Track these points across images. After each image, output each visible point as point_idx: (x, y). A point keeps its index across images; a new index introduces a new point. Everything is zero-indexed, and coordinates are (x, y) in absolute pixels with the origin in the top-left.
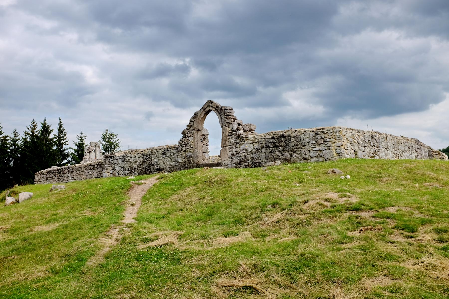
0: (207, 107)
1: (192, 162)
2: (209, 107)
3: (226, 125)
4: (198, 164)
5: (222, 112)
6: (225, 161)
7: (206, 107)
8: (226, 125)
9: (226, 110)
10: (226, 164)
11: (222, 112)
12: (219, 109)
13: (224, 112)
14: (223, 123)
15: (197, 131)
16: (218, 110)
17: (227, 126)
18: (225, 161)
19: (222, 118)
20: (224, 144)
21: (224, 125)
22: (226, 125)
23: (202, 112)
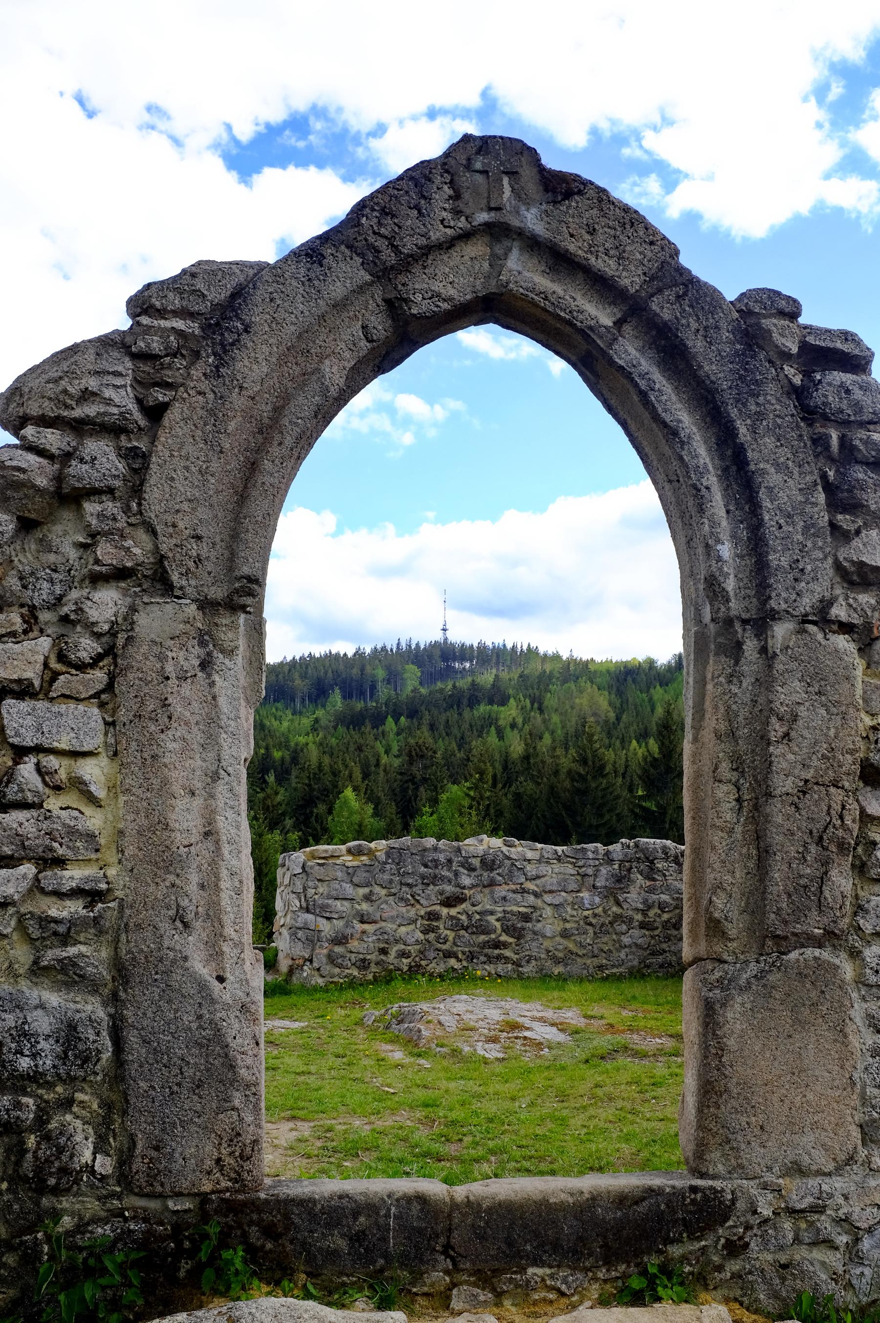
0: (448, 245)
1: (104, 1165)
2: (476, 249)
3: (839, 612)
4: (230, 1207)
5: (771, 389)
6: (798, 1170)
7: (438, 234)
8: (826, 605)
9: (838, 377)
10: (824, 1222)
11: (771, 389)
12: (708, 333)
13: (799, 394)
14: (778, 559)
15: (206, 605)
16: (696, 344)
17: (846, 628)
18: (798, 1170)
19: (774, 478)
20: (799, 912)
21: (806, 603)
22: (826, 605)
23: (340, 306)
